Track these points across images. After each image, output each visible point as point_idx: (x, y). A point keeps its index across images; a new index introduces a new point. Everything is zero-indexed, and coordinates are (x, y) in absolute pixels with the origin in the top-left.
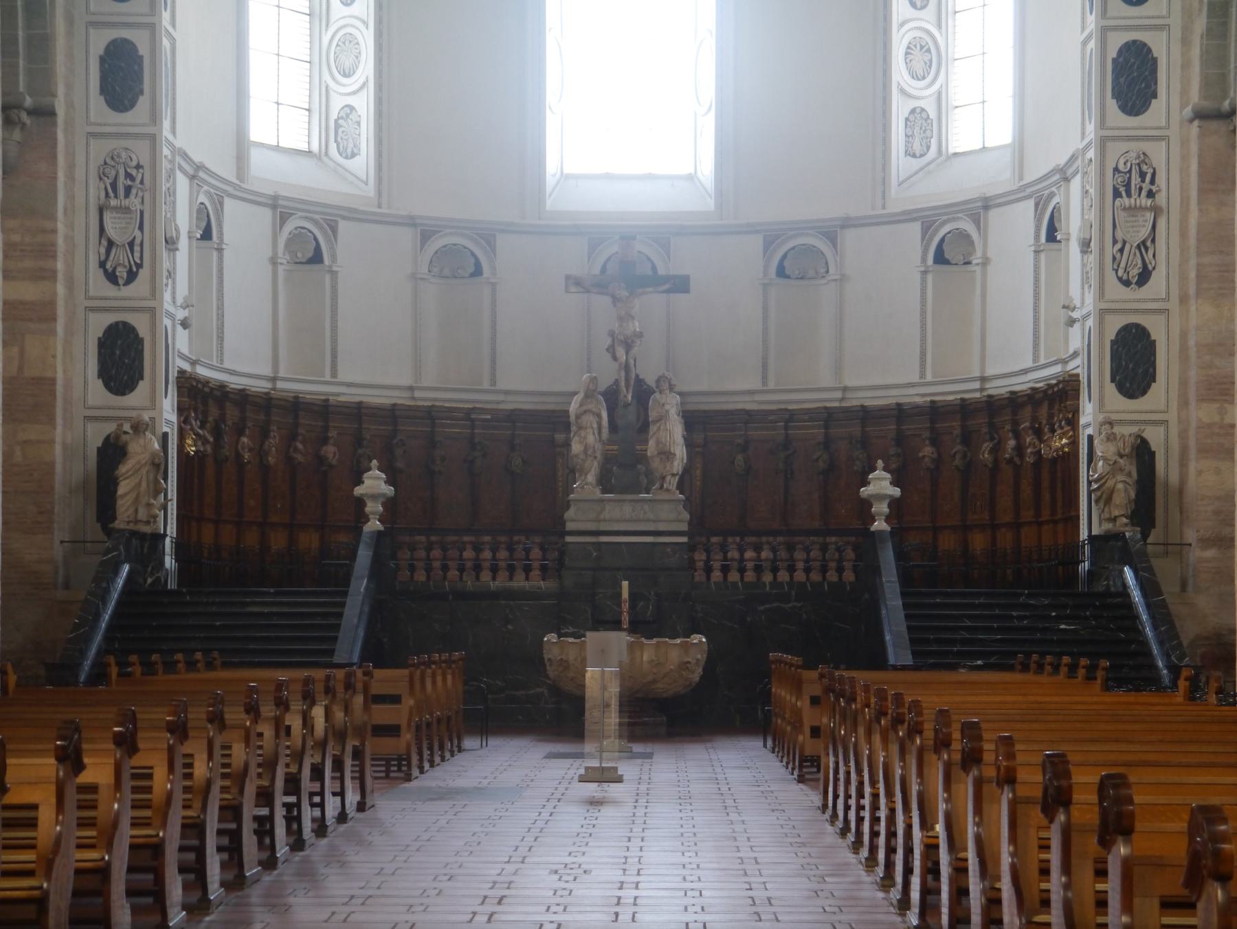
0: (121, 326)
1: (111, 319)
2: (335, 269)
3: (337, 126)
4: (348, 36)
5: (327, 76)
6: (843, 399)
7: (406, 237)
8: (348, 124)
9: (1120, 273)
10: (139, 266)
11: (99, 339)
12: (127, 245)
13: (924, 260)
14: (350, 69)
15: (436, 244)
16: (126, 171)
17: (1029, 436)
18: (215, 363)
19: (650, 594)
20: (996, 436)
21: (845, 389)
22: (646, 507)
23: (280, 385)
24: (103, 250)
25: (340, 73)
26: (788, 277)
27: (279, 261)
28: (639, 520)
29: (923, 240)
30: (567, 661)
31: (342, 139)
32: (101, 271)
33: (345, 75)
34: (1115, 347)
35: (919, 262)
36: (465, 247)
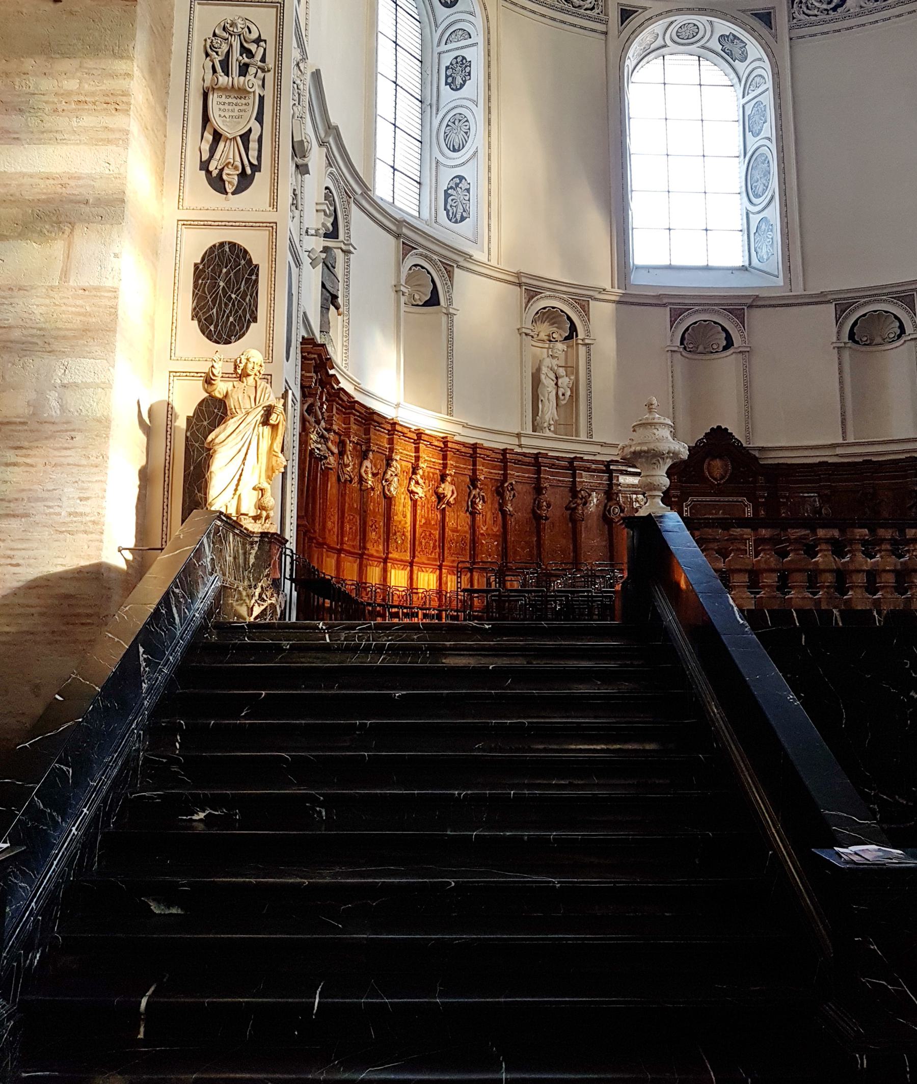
1: (214, 237)
2: (451, 311)
3: (447, 195)
4: (458, 117)
5: (436, 153)
8: (457, 192)
10: (256, 168)
11: (196, 265)
12: (239, 139)
14: (459, 144)
16: (242, 45)
24: (206, 147)
25: (449, 149)
26: (857, 343)
31: (451, 206)
33: (454, 150)
36: (562, 311)
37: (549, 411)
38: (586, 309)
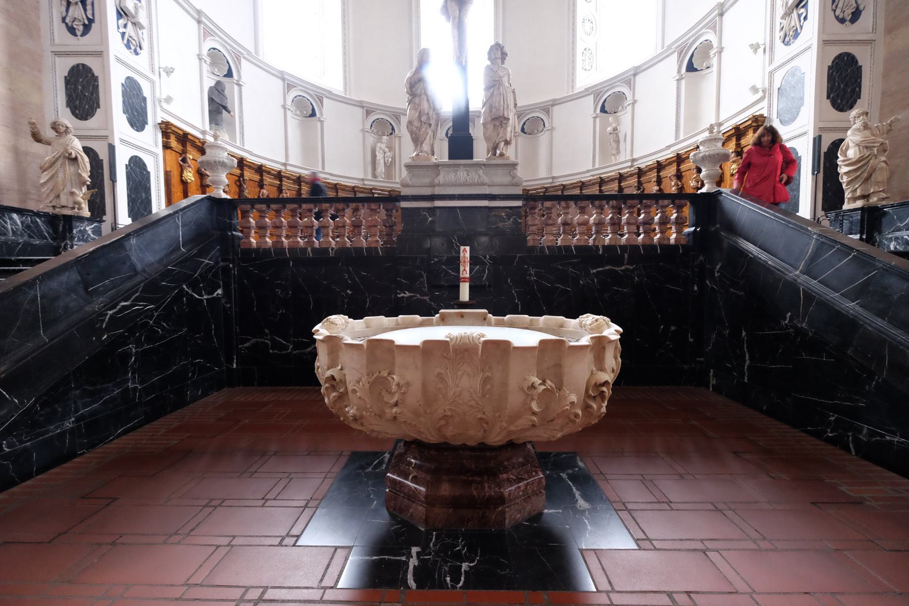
0: (81, 67)
2: (322, 119)
6: (552, 183)
7: (359, 112)
9: (838, 12)
10: (91, 21)
11: (65, 77)
13: (595, 111)
15: (373, 117)
17: (673, 181)
18: (238, 144)
19: (485, 257)
20: (642, 187)
21: (553, 178)
22: (481, 172)
23: (289, 168)
24: (64, 9)
26: (525, 133)
27: (287, 106)
28: (471, 185)
29: (594, 102)
30: (343, 382)
32: (64, 24)
34: (831, 71)
35: (592, 113)
37: (381, 168)
38: (399, 119)
